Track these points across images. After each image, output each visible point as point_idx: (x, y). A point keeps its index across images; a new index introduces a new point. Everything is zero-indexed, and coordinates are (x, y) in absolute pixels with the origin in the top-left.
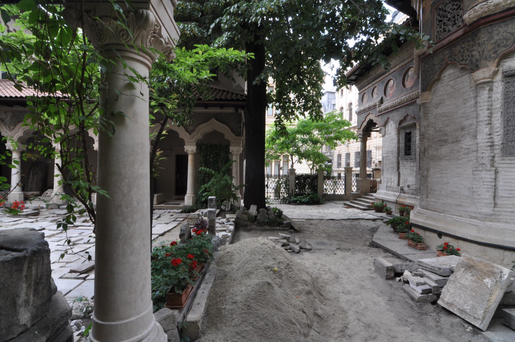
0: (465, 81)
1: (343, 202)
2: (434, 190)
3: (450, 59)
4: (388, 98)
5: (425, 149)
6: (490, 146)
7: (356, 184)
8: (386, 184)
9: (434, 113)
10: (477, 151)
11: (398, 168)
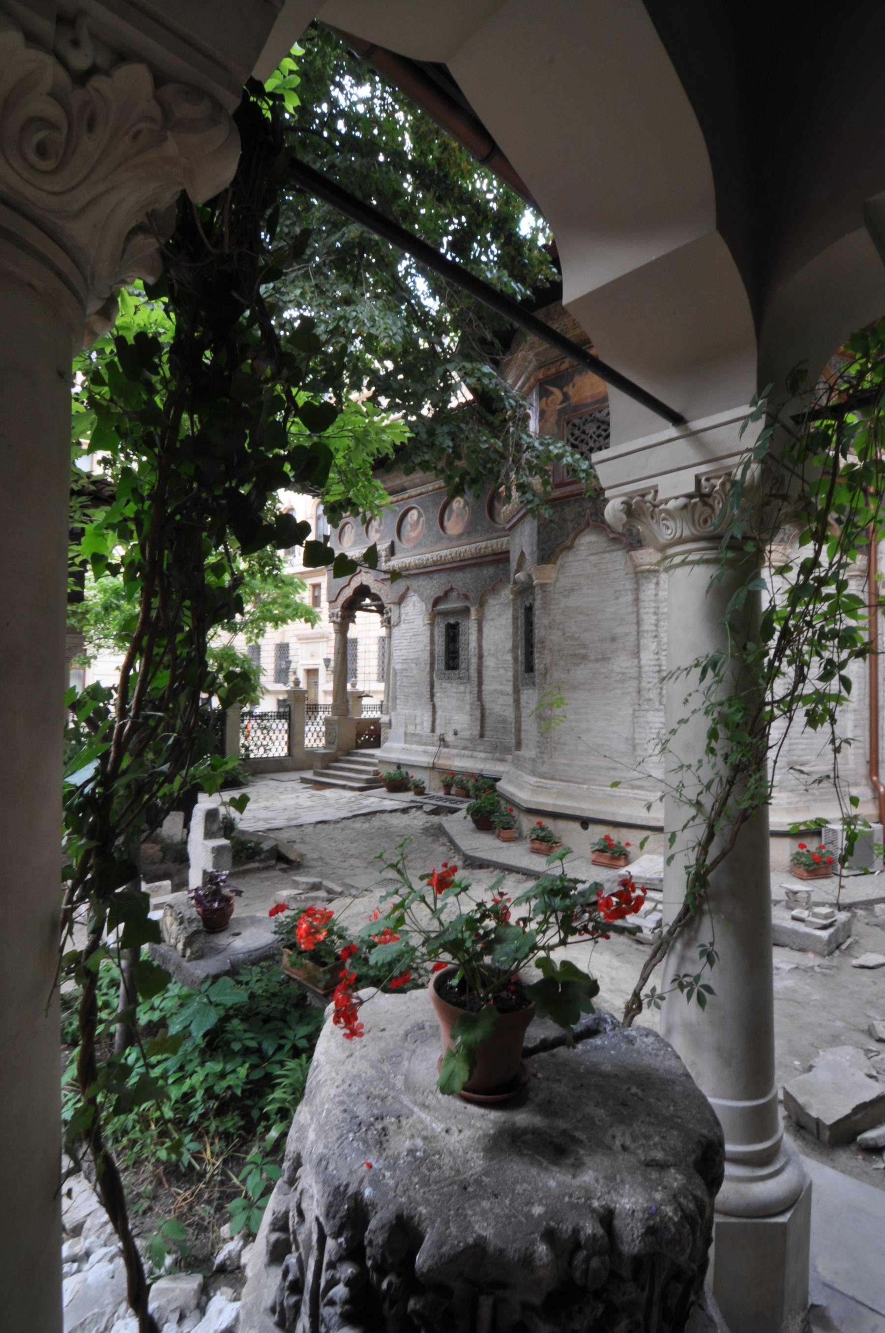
0: (617, 560)
1: (297, 775)
2: (564, 744)
3: (594, 518)
4: (406, 545)
5: (546, 669)
6: (659, 672)
7: (324, 729)
8: (403, 730)
9: (562, 605)
10: (639, 677)
11: (432, 696)
